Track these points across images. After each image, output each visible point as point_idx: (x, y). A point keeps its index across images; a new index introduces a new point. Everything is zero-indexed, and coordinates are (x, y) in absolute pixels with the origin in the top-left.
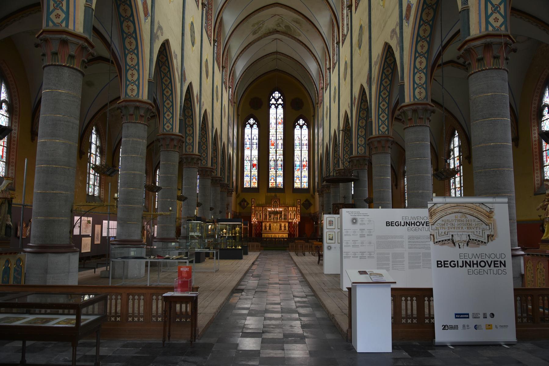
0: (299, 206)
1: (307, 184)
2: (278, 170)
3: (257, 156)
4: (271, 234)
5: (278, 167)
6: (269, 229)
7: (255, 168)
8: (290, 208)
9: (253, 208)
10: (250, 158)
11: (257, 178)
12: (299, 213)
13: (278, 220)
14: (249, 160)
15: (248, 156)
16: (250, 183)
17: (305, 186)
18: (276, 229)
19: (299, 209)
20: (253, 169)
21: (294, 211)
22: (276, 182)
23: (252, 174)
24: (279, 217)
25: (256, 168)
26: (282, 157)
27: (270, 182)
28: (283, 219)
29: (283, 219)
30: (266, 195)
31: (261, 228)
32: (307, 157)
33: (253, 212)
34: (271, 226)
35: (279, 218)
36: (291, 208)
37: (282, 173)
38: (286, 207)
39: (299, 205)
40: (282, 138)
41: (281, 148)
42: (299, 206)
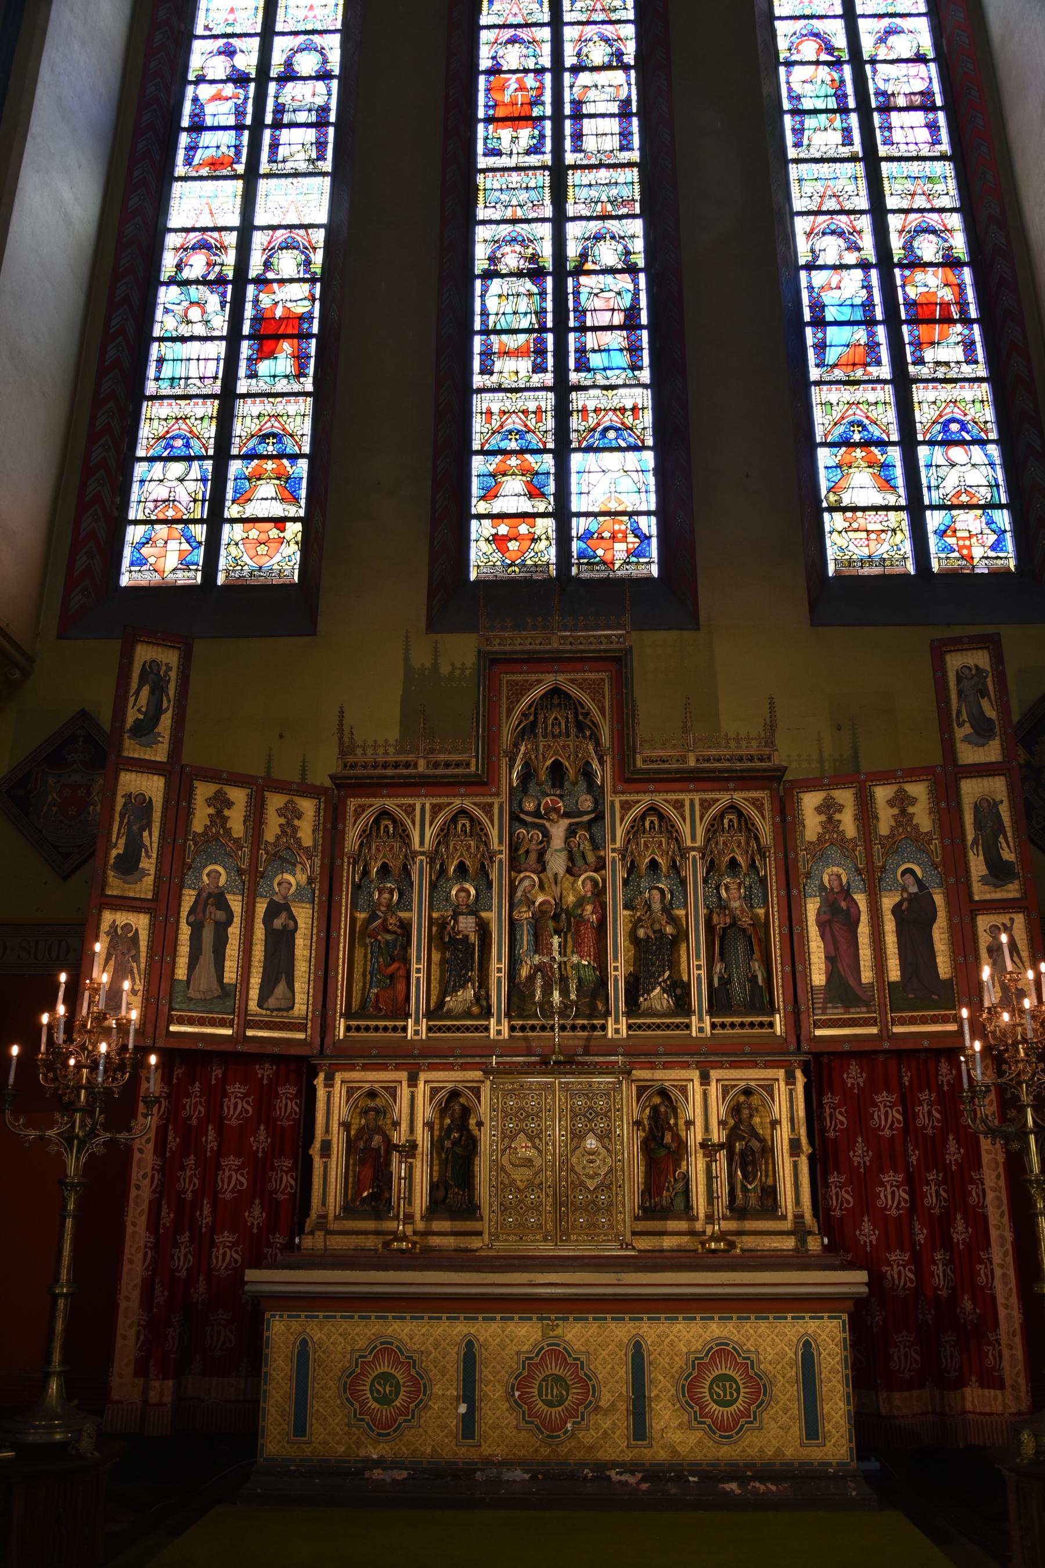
0: (991, 752)
1: (1003, 518)
2: (583, 366)
3: (319, 237)
4: (460, 1328)
5: (591, 340)
6: (435, 1209)
7: (283, 363)
8: (811, 800)
9: (153, 787)
10: (230, 258)
11: (302, 467)
12: (998, 872)
13: (617, 1028)
14: (221, 281)
15: (212, 237)
16: (200, 532)
17: (977, 552)
18: (563, 1205)
19: (986, 811)
20: (264, 367)
21: (892, 845)
22: (562, 514)
23: (239, 428)
24: (619, 969)
25: (300, 358)
26: (636, 226)
27: (480, 507)
28: (699, 996)
29: (699, 996)
30: (421, 658)
31: (285, 1181)
32: (955, 221)
33: (129, 865)
34: (471, 1145)
35: (635, 989)
36: (828, 808)
37: (643, 397)
38: (745, 780)
39: (983, 731)
40: (630, 49)
41: (613, 143)
42: (991, 752)
